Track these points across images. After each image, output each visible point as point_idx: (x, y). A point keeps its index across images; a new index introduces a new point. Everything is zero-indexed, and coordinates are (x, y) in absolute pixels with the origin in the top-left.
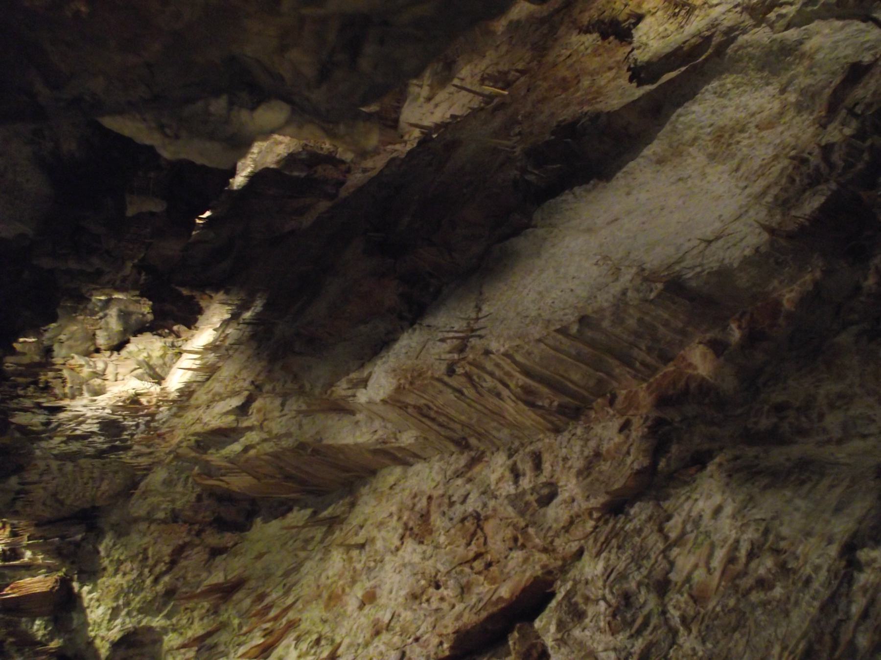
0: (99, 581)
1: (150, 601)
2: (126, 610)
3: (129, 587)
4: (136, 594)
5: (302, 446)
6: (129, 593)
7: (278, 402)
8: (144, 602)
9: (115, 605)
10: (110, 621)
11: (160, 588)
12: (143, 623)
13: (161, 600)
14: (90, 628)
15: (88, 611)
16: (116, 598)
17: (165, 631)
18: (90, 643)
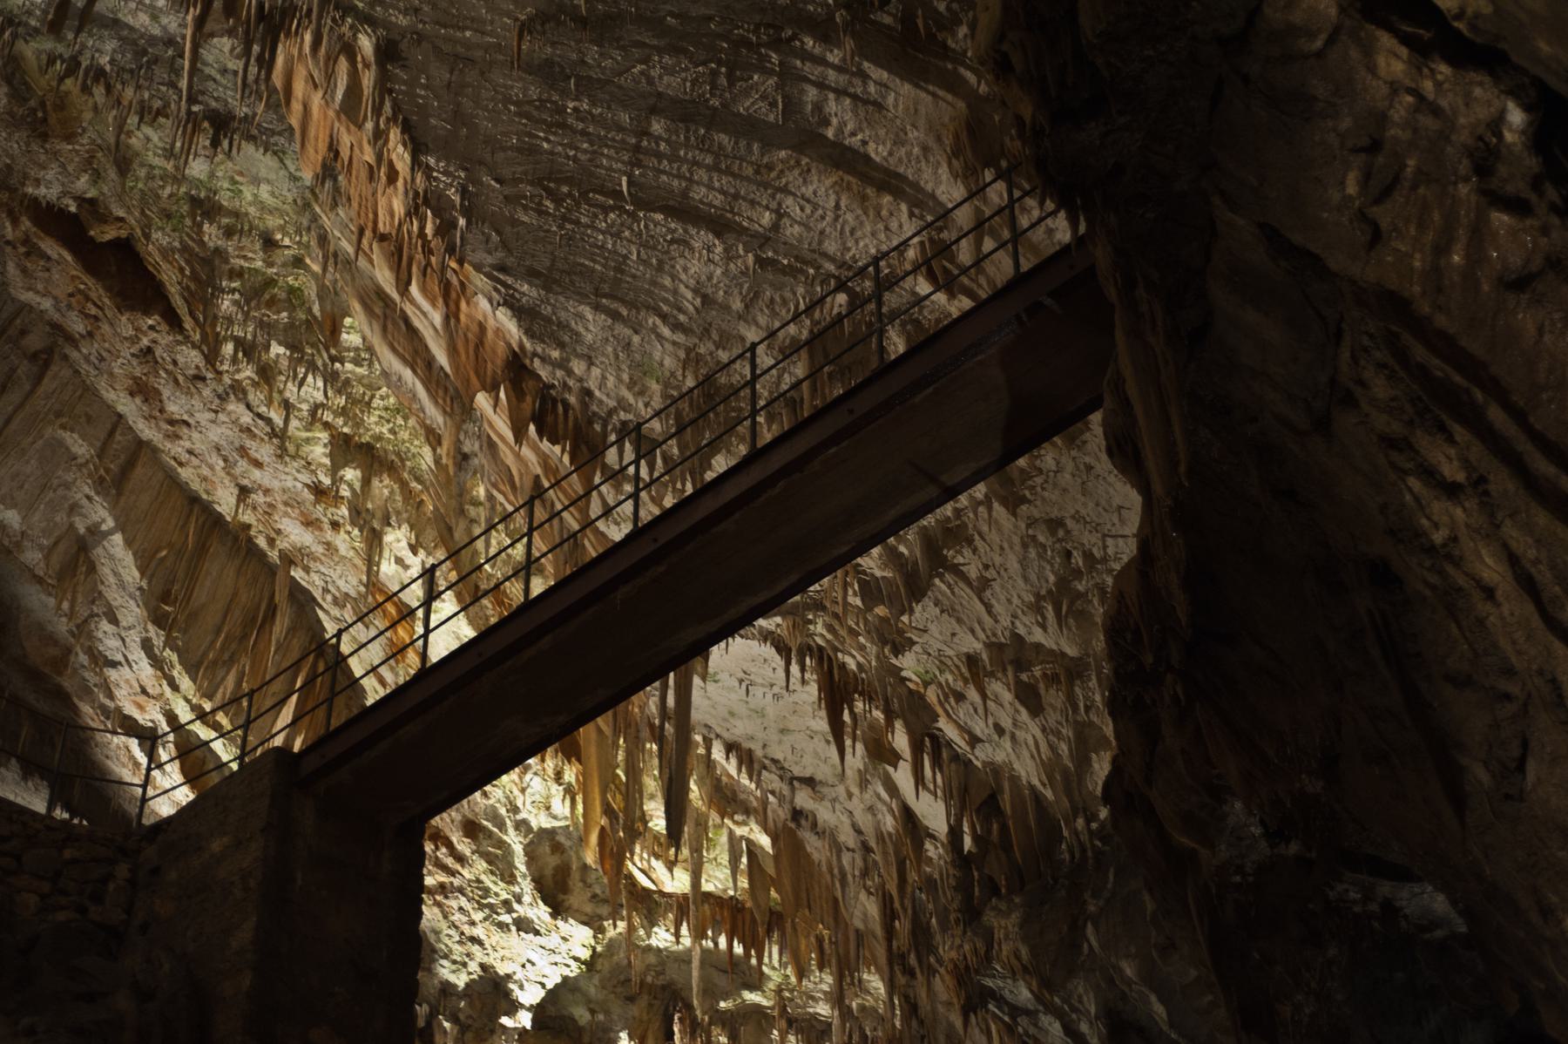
0: (501, 973)
1: (489, 862)
2: (516, 906)
3: (481, 907)
4: (487, 891)
5: (159, 620)
6: (491, 906)
7: (112, 674)
8: (492, 873)
9: (513, 928)
10: (537, 933)
11: (464, 846)
12: (523, 868)
13: (485, 843)
14: (567, 972)
15: (550, 986)
16: (502, 926)
17: (522, 826)
18: (590, 965)
